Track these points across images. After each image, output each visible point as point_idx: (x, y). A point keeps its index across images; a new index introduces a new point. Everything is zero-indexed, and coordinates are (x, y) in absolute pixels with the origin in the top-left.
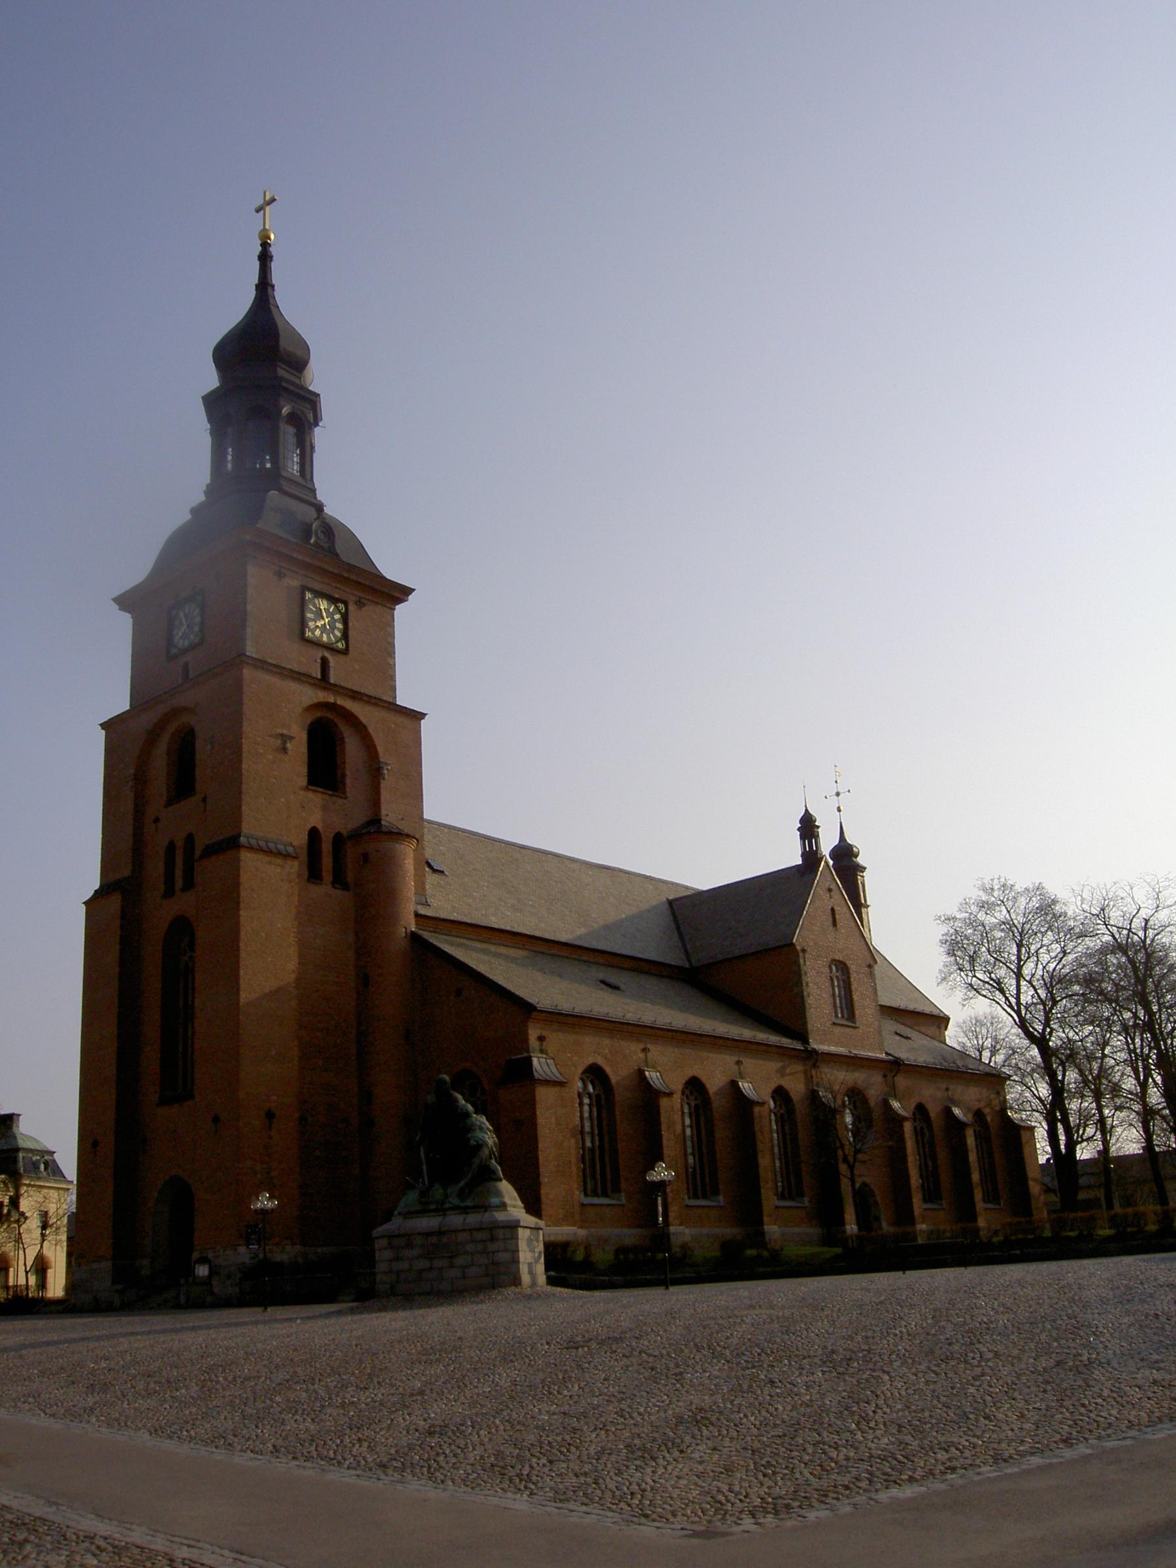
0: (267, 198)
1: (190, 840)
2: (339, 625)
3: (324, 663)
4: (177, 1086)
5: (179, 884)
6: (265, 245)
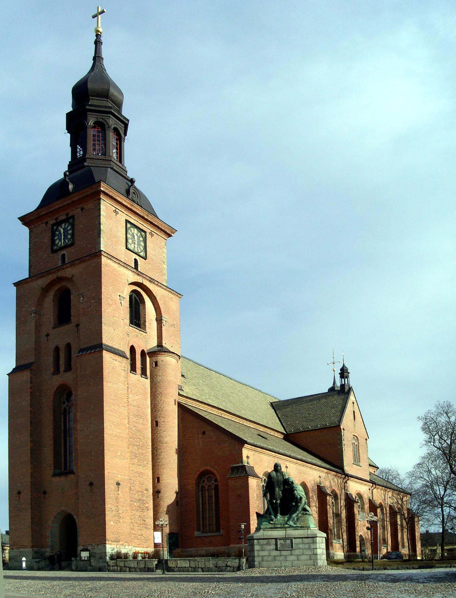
0: (100, 11)
1: (68, 347)
2: (143, 244)
3: (136, 260)
4: (63, 467)
5: (62, 368)
6: (98, 36)
